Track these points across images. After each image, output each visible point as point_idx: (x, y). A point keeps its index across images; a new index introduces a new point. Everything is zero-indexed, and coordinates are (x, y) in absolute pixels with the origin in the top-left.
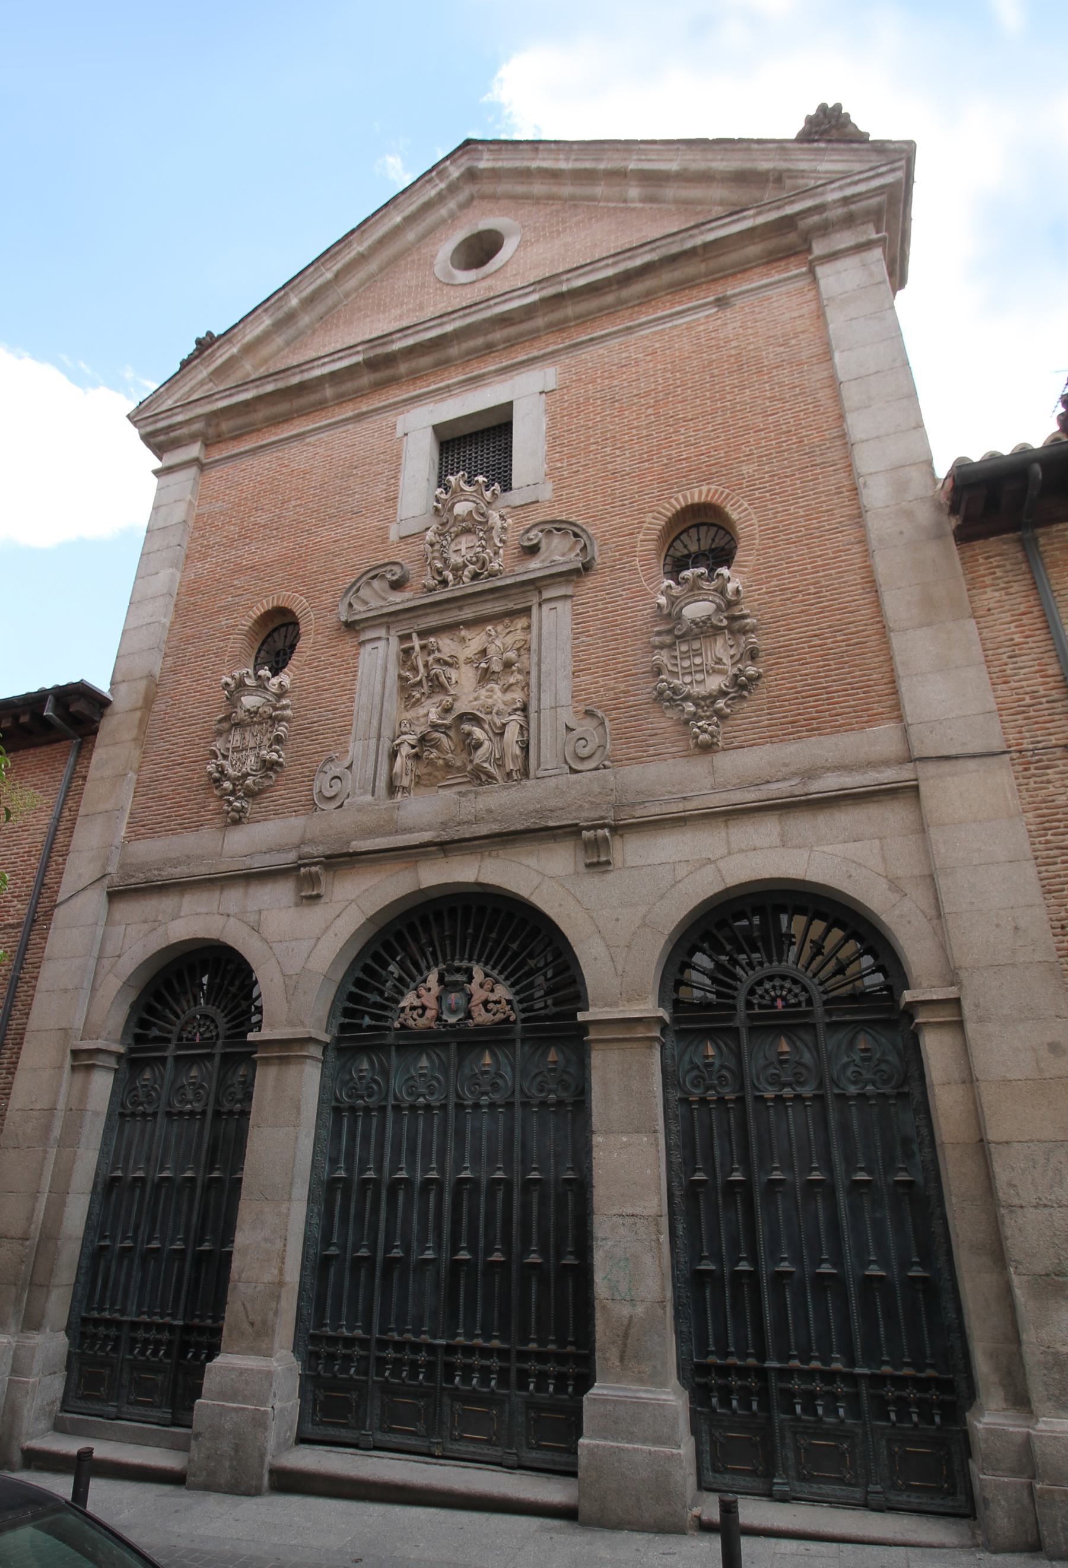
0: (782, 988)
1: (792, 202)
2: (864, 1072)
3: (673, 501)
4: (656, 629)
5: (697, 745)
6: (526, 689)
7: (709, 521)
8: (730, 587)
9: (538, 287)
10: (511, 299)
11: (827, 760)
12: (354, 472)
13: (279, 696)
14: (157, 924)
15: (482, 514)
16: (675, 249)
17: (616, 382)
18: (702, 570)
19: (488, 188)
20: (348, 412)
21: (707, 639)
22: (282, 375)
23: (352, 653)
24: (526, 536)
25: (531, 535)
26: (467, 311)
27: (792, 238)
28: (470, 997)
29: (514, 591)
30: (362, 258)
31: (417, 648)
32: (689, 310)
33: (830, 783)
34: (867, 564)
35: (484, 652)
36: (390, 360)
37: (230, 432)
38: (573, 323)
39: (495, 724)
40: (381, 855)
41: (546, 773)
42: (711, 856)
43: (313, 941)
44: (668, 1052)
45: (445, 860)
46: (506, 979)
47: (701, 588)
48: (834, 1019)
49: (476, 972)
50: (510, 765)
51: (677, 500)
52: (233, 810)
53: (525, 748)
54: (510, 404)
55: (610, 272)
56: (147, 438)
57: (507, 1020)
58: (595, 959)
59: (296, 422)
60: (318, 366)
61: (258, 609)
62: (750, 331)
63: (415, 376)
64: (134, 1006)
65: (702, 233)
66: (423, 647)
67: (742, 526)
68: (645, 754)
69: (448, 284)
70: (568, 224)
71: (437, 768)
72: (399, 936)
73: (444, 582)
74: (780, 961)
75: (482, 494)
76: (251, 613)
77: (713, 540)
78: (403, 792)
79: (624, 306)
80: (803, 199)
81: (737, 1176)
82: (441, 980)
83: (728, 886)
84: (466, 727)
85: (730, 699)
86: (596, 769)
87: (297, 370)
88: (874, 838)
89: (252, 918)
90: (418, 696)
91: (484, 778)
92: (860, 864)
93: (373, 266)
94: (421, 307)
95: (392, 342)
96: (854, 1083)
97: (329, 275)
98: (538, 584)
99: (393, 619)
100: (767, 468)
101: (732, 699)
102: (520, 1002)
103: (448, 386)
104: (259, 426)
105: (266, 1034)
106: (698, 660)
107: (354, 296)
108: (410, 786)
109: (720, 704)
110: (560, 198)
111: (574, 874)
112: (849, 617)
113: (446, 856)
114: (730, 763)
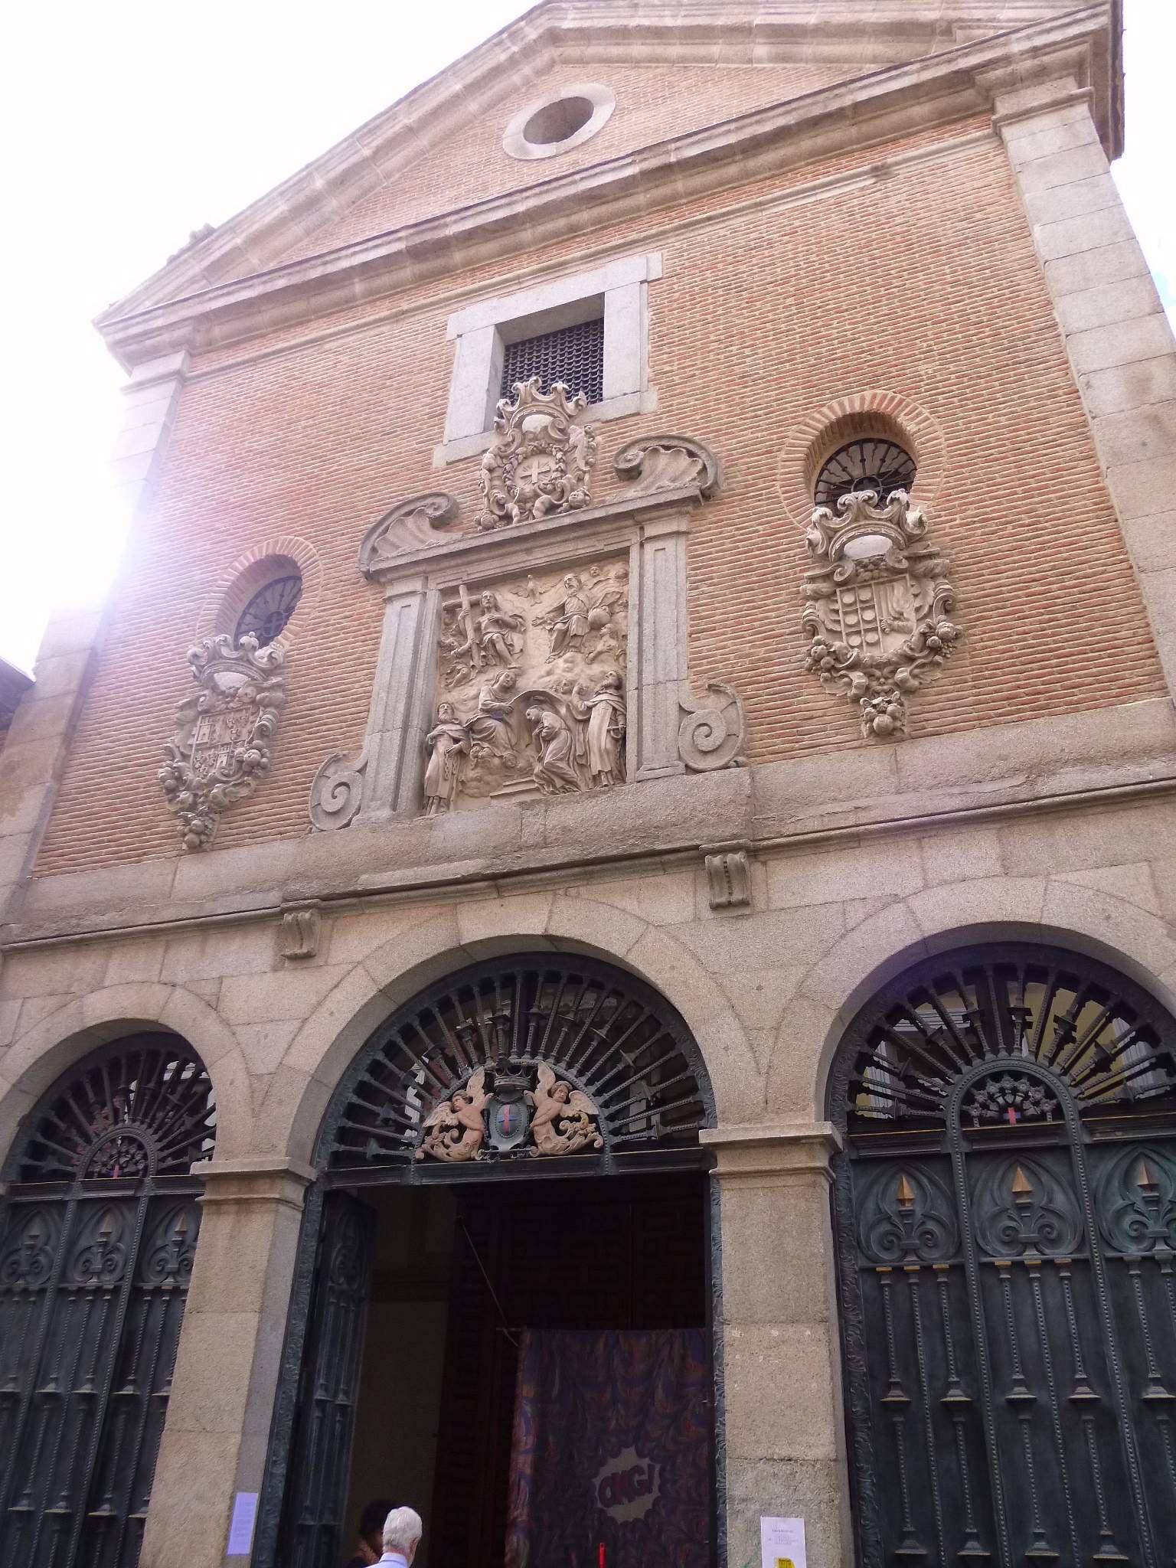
0: (1015, 1091)
1: (966, 55)
2: (1150, 1223)
3: (825, 410)
4: (806, 574)
5: (872, 731)
6: (621, 659)
7: (876, 436)
8: (911, 517)
9: (638, 158)
10: (602, 173)
11: (1063, 750)
12: (388, 383)
13: (267, 673)
14: (69, 997)
15: (561, 431)
16: (817, 111)
17: (743, 268)
18: (869, 493)
19: (573, 51)
20: (383, 310)
21: (881, 587)
22: (298, 268)
23: (373, 614)
24: (622, 457)
25: (629, 454)
26: (545, 188)
27: (968, 96)
28: (533, 1111)
29: (605, 527)
30: (411, 131)
31: (466, 605)
32: (838, 181)
33: (1070, 781)
34: (1100, 485)
35: (562, 608)
36: (443, 246)
37: (223, 339)
38: (684, 201)
39: (576, 708)
40: (404, 894)
41: (651, 774)
42: (898, 891)
43: (297, 1024)
44: (842, 1194)
45: (498, 902)
46: (589, 1083)
47: (867, 517)
48: (1098, 1137)
49: (543, 1073)
50: (596, 764)
51: (831, 408)
52: (191, 831)
53: (620, 740)
54: (601, 296)
55: (732, 139)
57: (589, 1147)
58: (726, 1049)
59: (313, 325)
60: (346, 256)
61: (246, 558)
62: (920, 204)
63: (473, 267)
64: (24, 1123)
65: (851, 92)
66: (474, 605)
67: (922, 440)
68: (797, 745)
69: (520, 160)
70: (676, 89)
71: (490, 771)
72: (426, 1018)
73: (507, 518)
74: (1010, 1050)
75: (562, 406)
76: (236, 564)
77: (883, 460)
78: (439, 806)
79: (752, 179)
80: (981, 51)
81: (956, 1396)
82: (488, 1087)
83: (926, 935)
84: (532, 712)
85: (917, 667)
86: (726, 767)
87: (319, 261)
88: (1139, 861)
89: (209, 989)
90: (465, 670)
91: (559, 783)
92: (1122, 899)
93: (423, 141)
94: (485, 187)
95: (446, 225)
96: (1137, 1239)
98: (639, 518)
99: (434, 567)
100: (952, 367)
101: (923, 666)
102: (611, 1118)
103: (518, 277)
104: (264, 331)
105: (218, 1165)
106: (869, 615)
107: (397, 176)
108: (449, 797)
109: (903, 673)
110: (666, 60)
111: (693, 920)
112: (1080, 555)
113: (500, 896)
114: (920, 757)
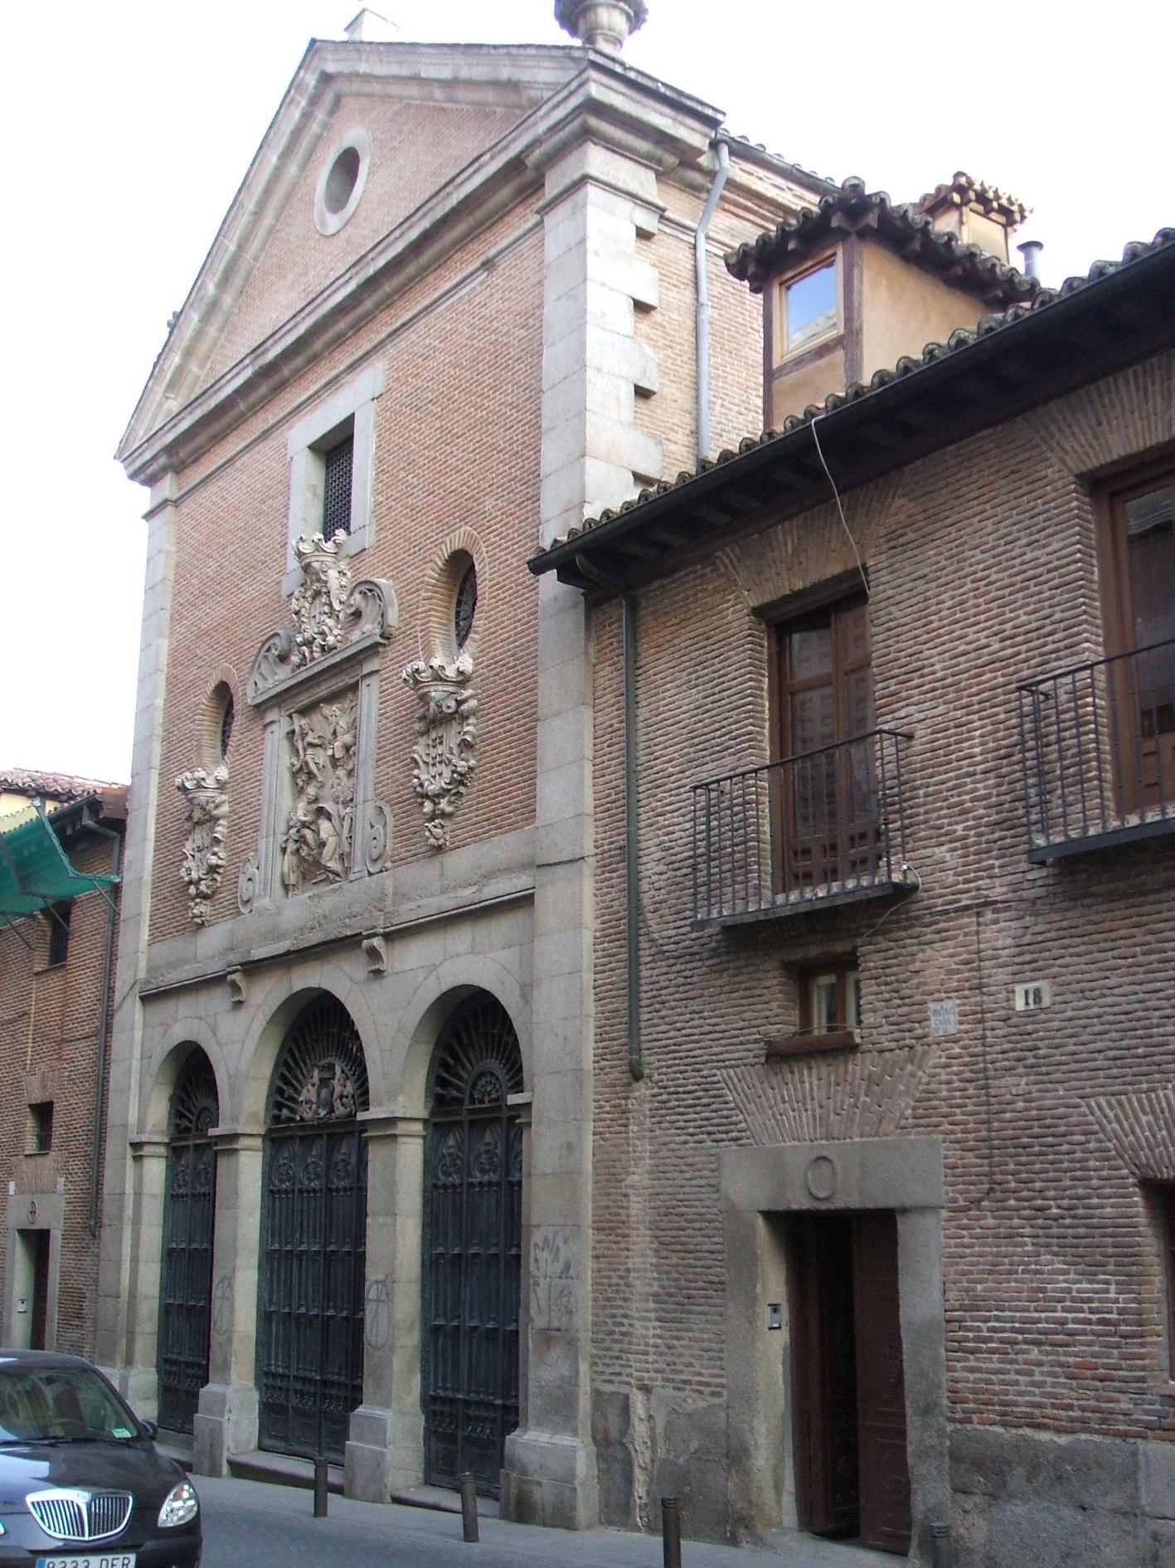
16: (440, 212)
55: (399, 247)
56: (133, 476)
59: (231, 438)
60: (225, 384)
95: (268, 350)
97: (232, 247)
114: (458, 862)
